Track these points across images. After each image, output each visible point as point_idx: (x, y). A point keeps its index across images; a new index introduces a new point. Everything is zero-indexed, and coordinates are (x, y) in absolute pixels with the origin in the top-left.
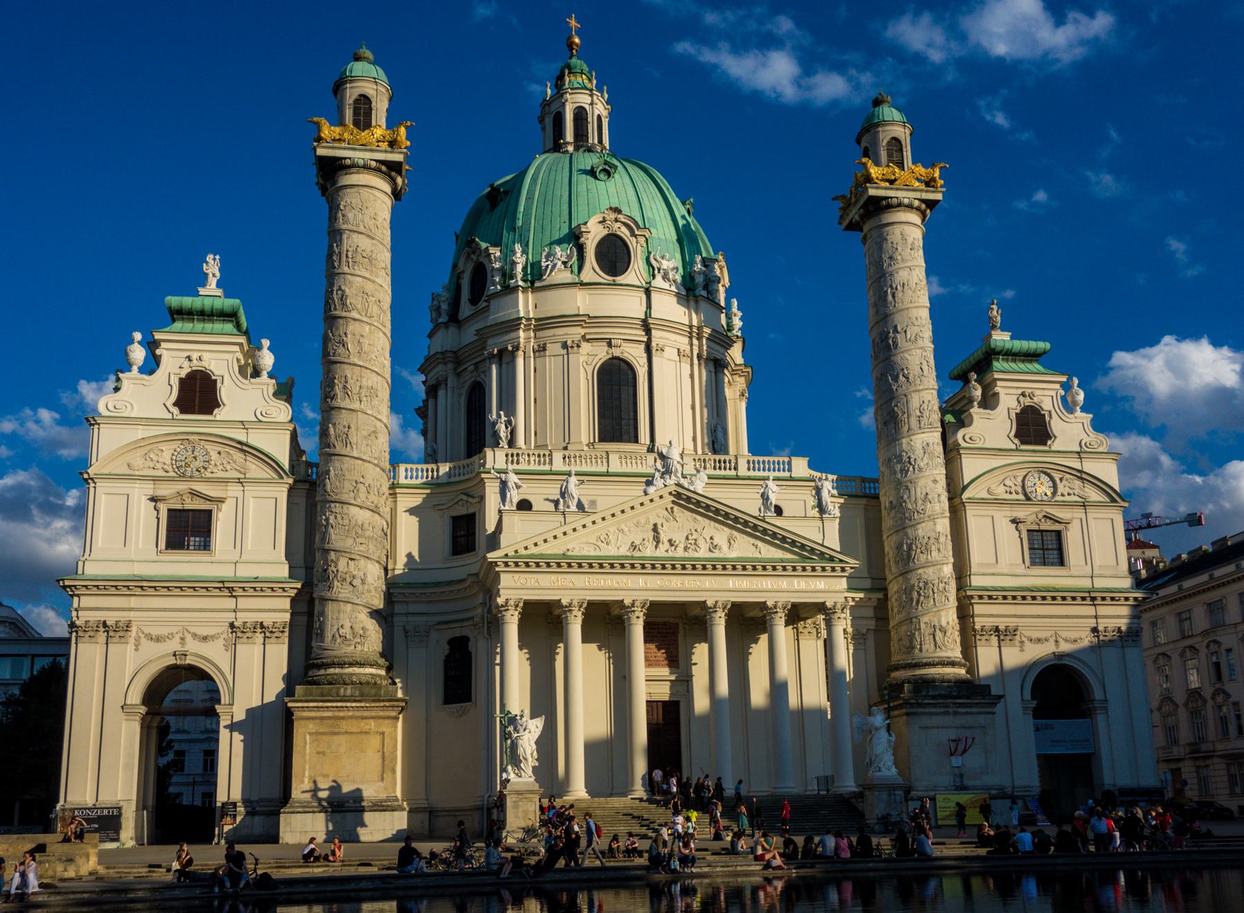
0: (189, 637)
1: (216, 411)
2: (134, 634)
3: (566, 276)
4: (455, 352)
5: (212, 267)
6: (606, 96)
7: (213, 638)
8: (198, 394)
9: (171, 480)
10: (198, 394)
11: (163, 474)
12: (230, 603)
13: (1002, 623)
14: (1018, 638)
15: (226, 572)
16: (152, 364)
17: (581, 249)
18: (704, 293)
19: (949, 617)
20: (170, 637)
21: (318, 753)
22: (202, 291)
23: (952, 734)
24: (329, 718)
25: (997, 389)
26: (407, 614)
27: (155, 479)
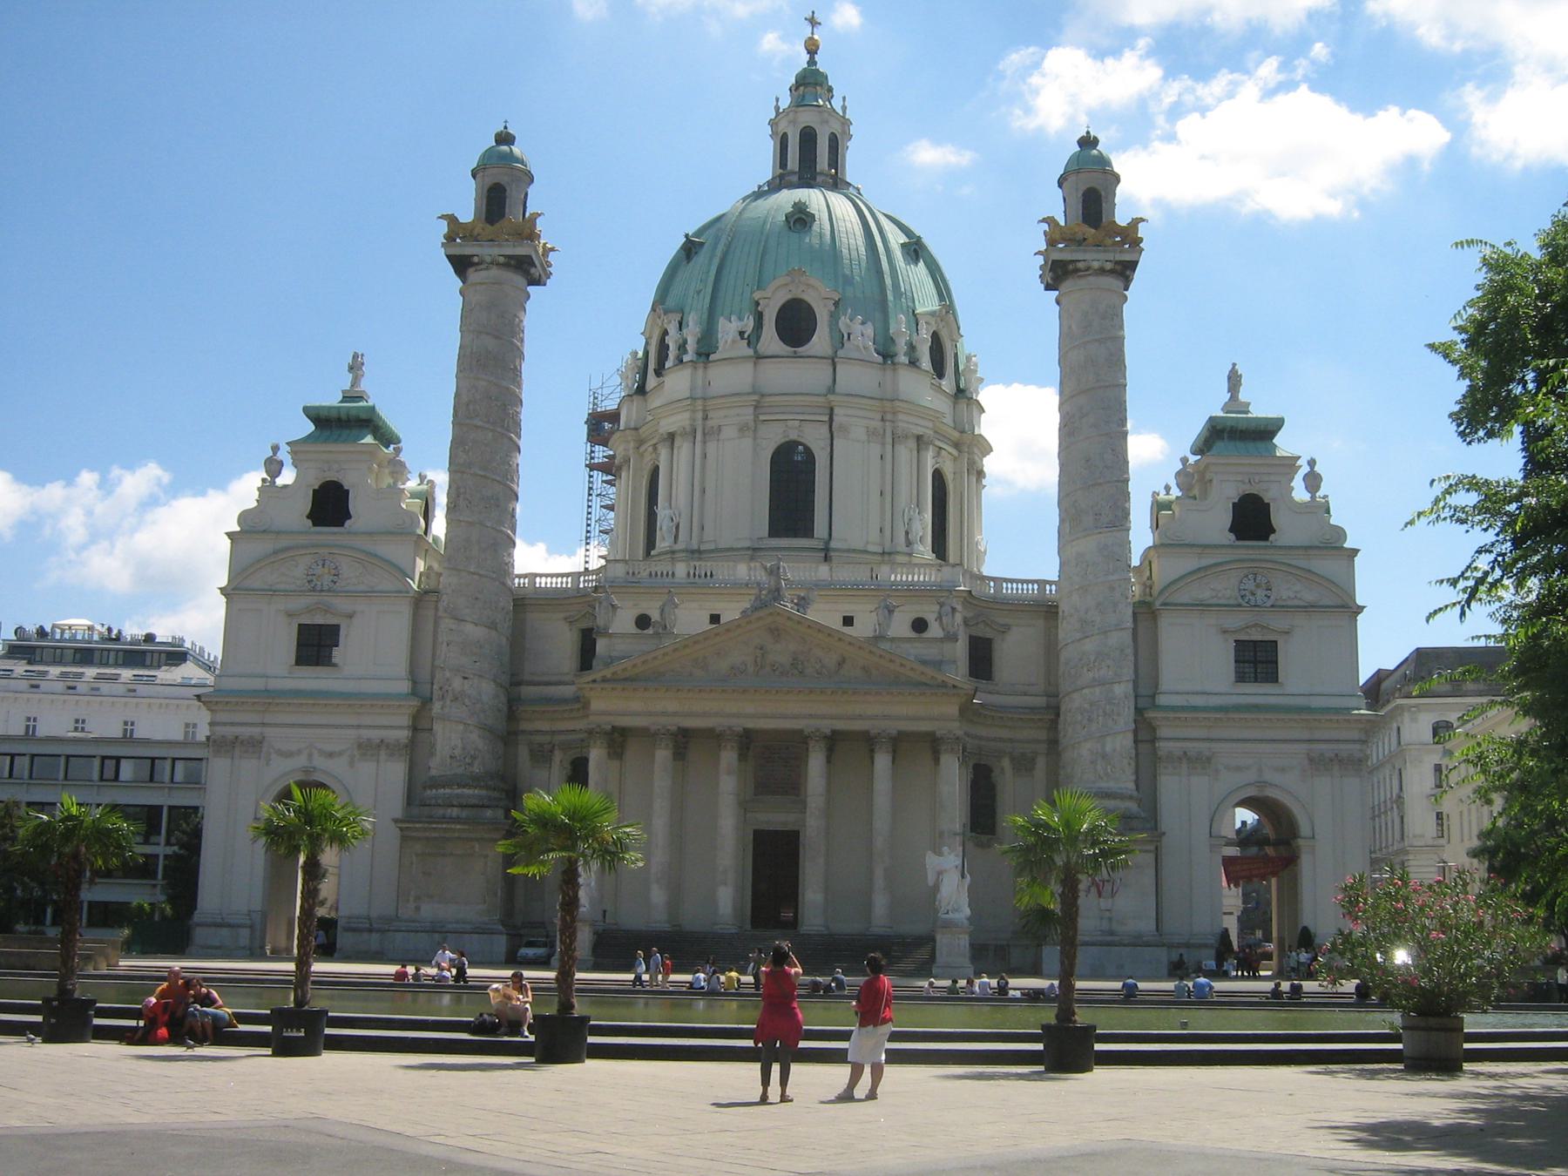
3: (743, 349)
4: (636, 429)
7: (340, 754)
10: (330, 505)
15: (350, 686)
17: (759, 318)
18: (904, 359)
19: (1121, 743)
20: (299, 752)
26: (531, 733)
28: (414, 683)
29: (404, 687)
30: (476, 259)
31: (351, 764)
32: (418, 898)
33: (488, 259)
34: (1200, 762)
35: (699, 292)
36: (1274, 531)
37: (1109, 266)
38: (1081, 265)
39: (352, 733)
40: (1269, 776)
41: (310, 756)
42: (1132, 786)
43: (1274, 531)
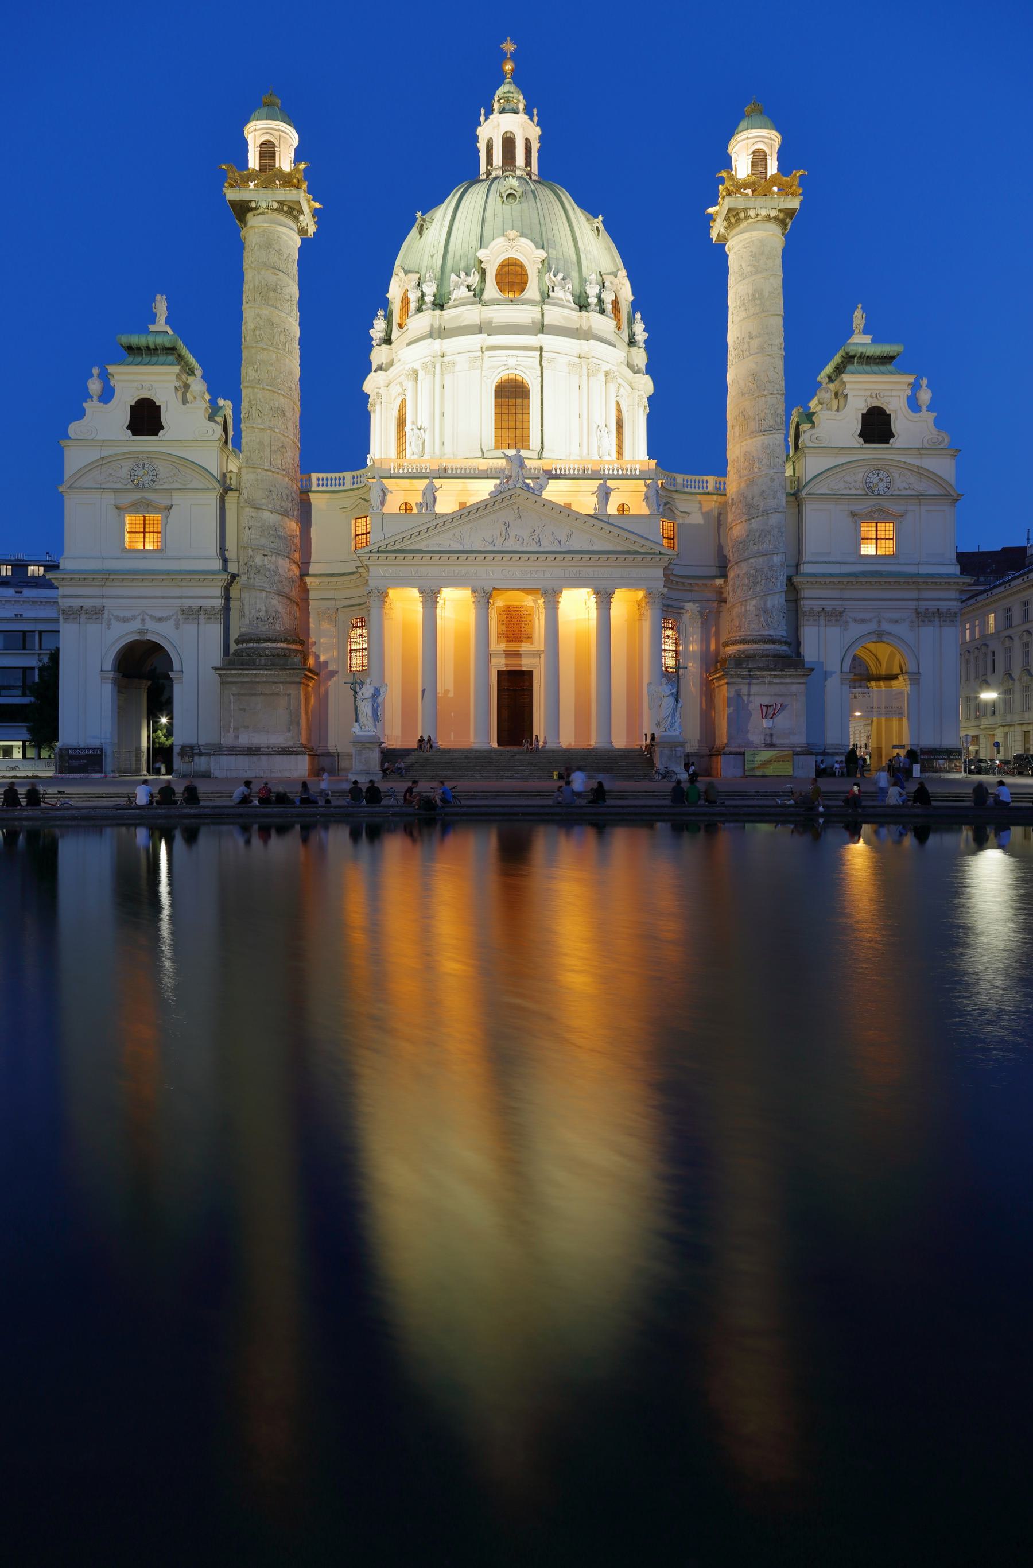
0: (147, 618)
1: (161, 433)
2: (105, 616)
5: (161, 307)
6: (536, 119)
7: (168, 618)
8: (146, 418)
9: (128, 491)
11: (118, 486)
12: (178, 592)
13: (829, 605)
14: (843, 619)
16: (107, 395)
17: (483, 272)
20: (134, 618)
21: (241, 709)
22: (152, 328)
23: (765, 701)
24: (248, 682)
25: (846, 392)
27: (116, 491)
28: (225, 561)
29: (216, 565)
30: (253, 205)
31: (177, 626)
32: (236, 729)
33: (264, 205)
34: (833, 616)
35: (432, 256)
36: (893, 436)
37: (774, 213)
38: (752, 213)
39: (178, 602)
40: (886, 627)
41: (143, 620)
42: (784, 633)
43: (893, 436)
